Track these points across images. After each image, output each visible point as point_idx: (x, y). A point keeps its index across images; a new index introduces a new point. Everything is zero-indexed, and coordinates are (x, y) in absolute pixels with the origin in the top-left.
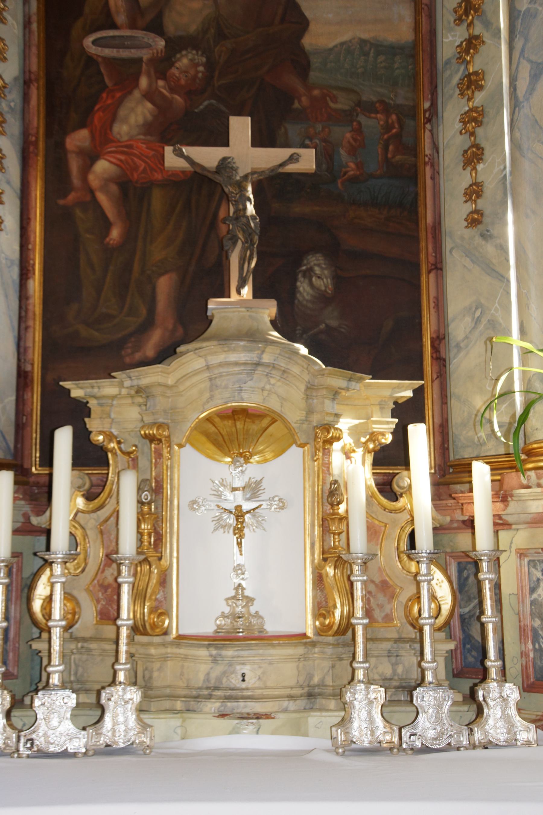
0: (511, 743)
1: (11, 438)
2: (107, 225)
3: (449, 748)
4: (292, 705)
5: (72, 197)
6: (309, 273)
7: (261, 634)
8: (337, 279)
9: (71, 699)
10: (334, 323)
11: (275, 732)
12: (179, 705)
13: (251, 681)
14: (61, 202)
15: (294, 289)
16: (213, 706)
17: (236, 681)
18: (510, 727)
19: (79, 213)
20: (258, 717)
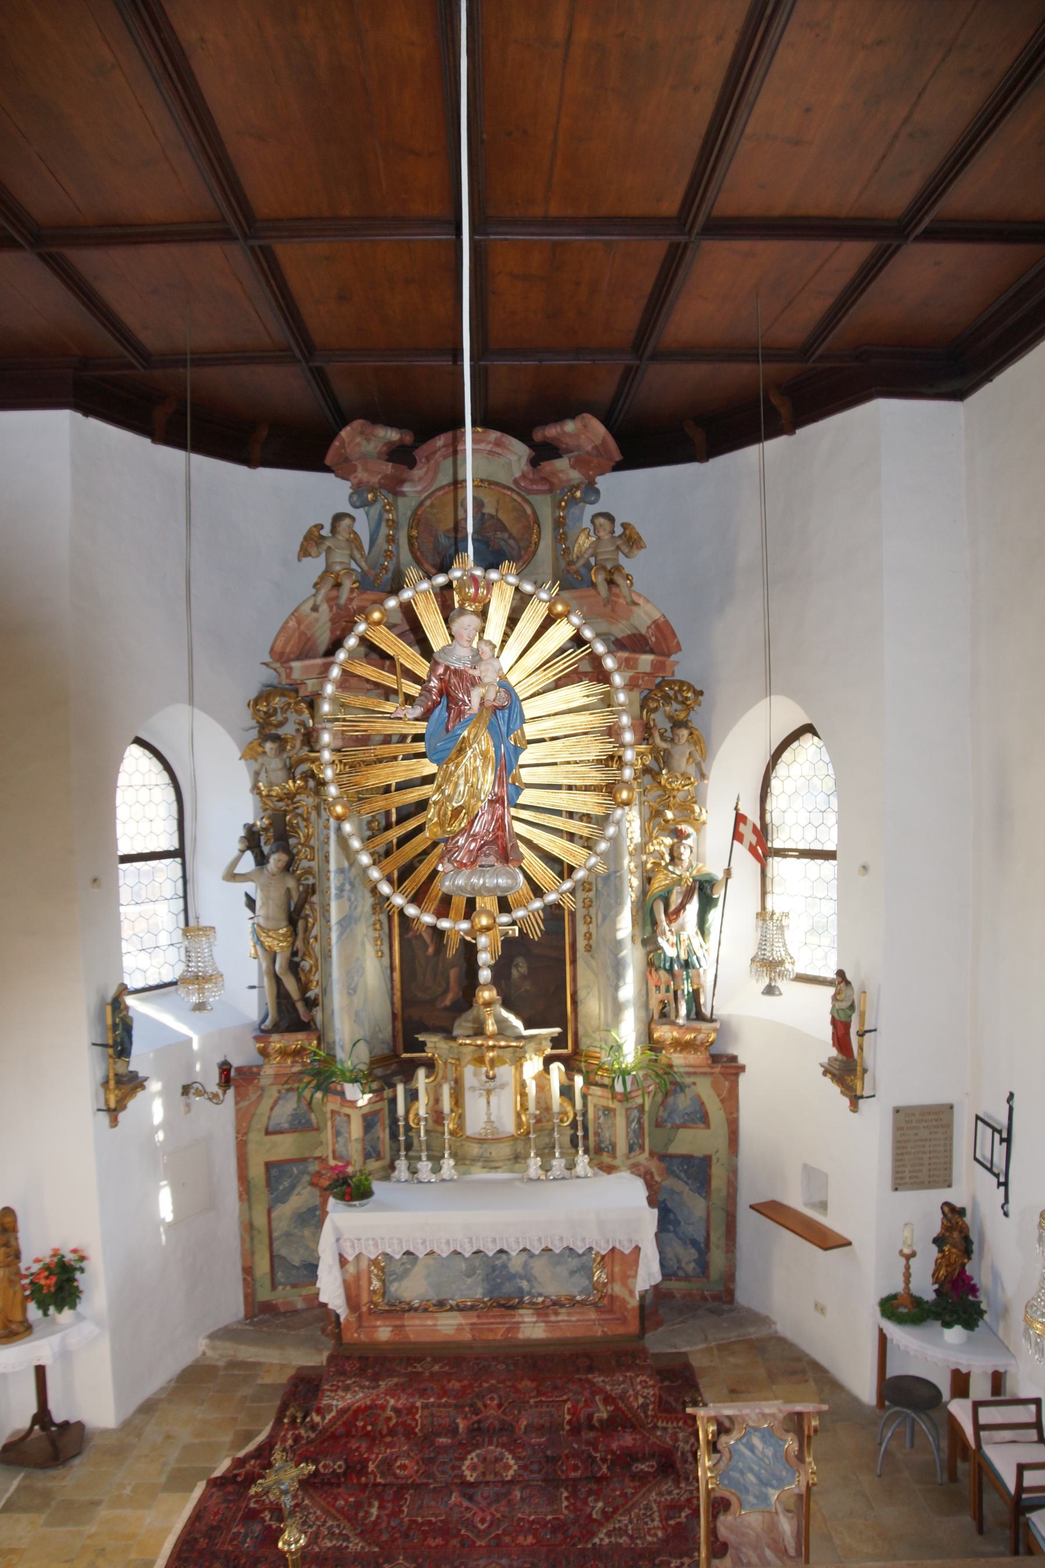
0: (586, 1177)
1: (391, 1044)
2: (426, 946)
3: (563, 1178)
4: (508, 1163)
5: (411, 934)
6: (517, 966)
7: (496, 1137)
8: (529, 968)
9: (430, 1165)
10: (528, 988)
11: (504, 1172)
12: (468, 1162)
13: (494, 1154)
14: (406, 936)
15: (510, 973)
16: (480, 1164)
17: (487, 1154)
18: (585, 1169)
19: (414, 942)
20: (496, 1168)
